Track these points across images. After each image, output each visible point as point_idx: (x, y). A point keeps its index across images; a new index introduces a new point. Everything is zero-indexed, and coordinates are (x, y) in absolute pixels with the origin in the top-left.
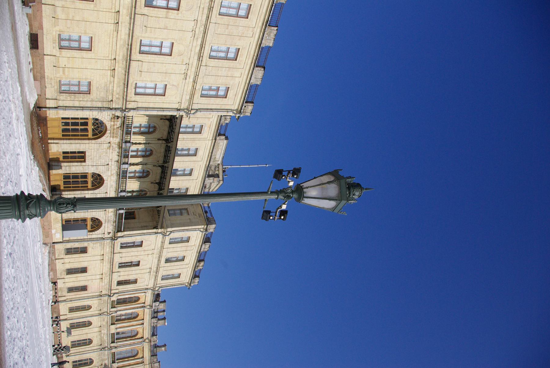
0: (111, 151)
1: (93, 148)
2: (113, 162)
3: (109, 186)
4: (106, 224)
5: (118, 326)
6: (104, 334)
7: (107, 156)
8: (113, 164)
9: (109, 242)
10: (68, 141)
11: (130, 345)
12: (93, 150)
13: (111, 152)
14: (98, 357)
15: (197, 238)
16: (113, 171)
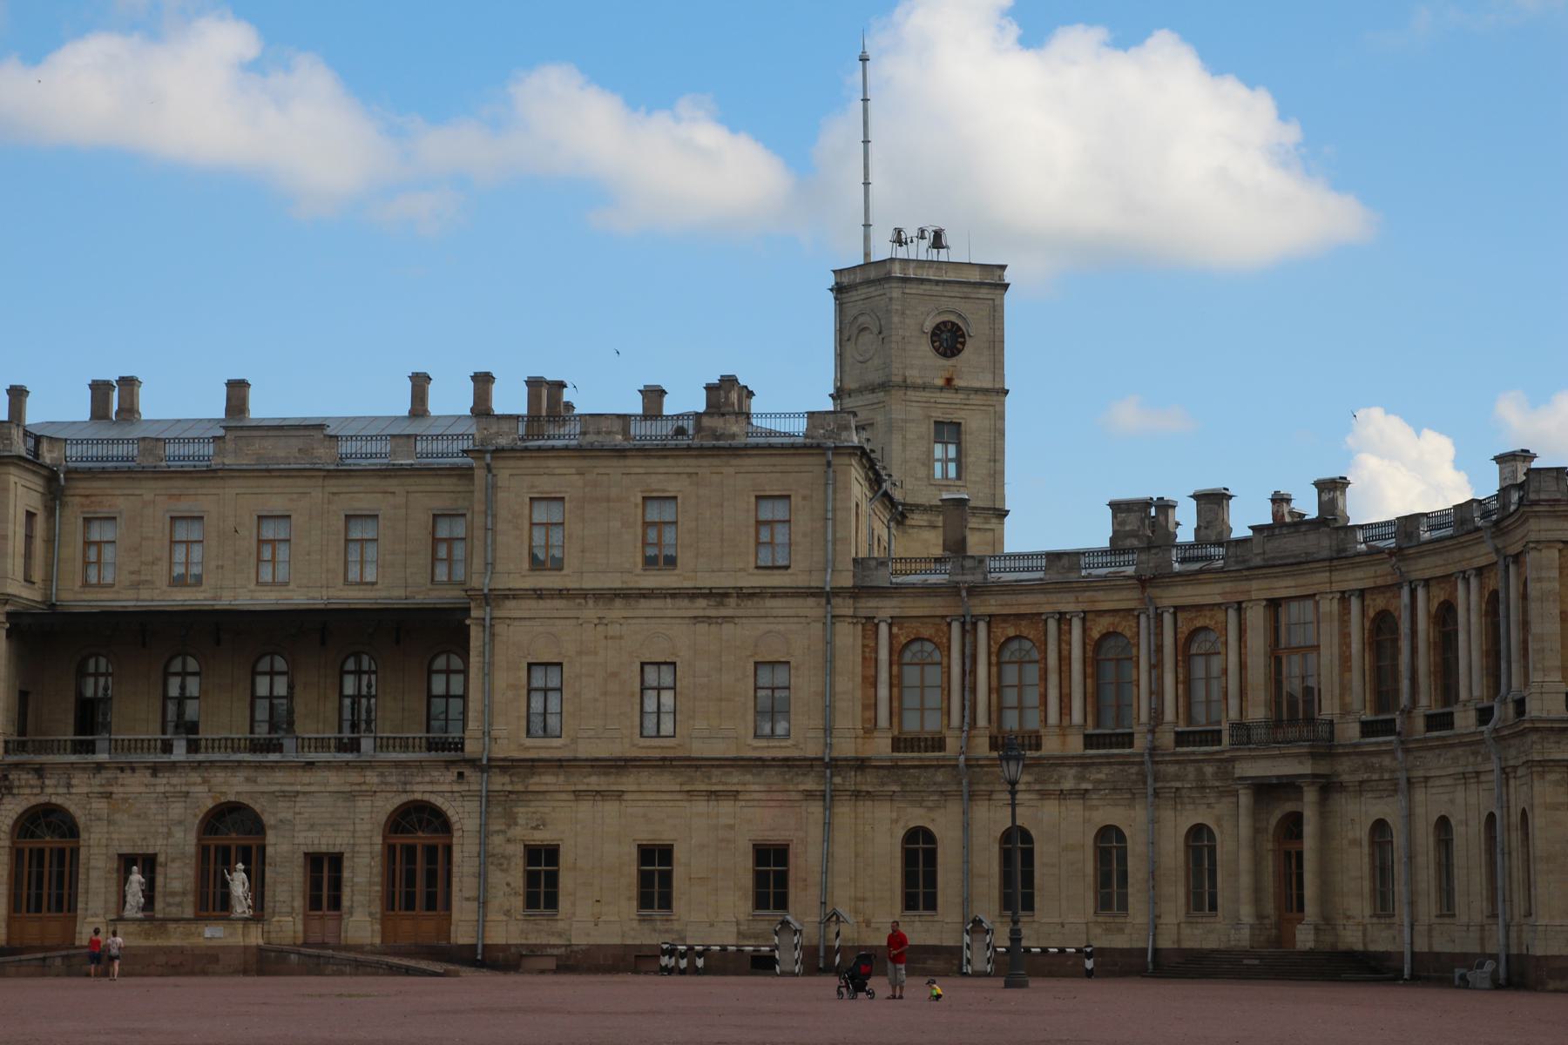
0: (115, 789)
1: (106, 836)
2: (158, 781)
3: (247, 788)
4: (415, 788)
5: (1053, 717)
6: (1082, 779)
7: (136, 798)
8: (164, 781)
9: (511, 776)
10: (81, 899)
11: (1156, 666)
12: (115, 836)
13: (121, 789)
14: (1188, 807)
15: (542, 471)
16: (192, 780)
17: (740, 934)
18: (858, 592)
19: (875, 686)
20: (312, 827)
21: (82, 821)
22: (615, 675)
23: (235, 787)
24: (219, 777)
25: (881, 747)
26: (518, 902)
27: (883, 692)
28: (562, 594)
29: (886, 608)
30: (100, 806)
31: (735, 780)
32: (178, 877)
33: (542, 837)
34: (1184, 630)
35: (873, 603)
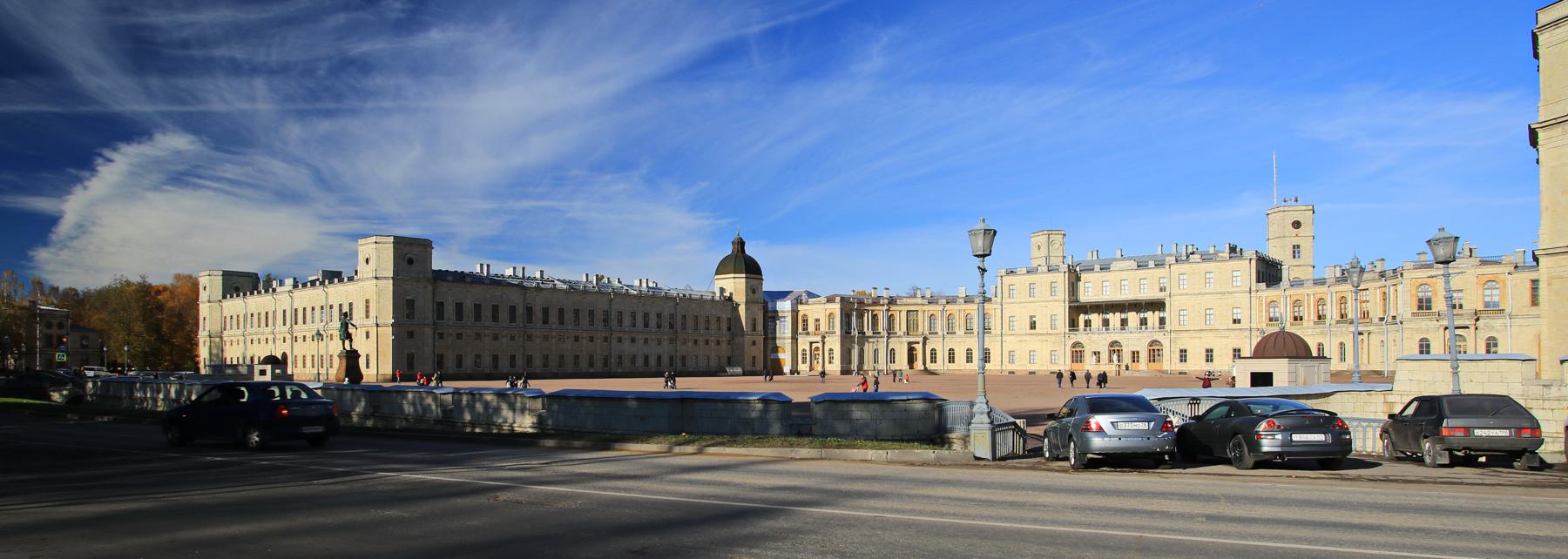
21: (1085, 345)
26: (1178, 361)
30: (1088, 341)
31: (1227, 333)
32: (1104, 356)
33: (1183, 347)
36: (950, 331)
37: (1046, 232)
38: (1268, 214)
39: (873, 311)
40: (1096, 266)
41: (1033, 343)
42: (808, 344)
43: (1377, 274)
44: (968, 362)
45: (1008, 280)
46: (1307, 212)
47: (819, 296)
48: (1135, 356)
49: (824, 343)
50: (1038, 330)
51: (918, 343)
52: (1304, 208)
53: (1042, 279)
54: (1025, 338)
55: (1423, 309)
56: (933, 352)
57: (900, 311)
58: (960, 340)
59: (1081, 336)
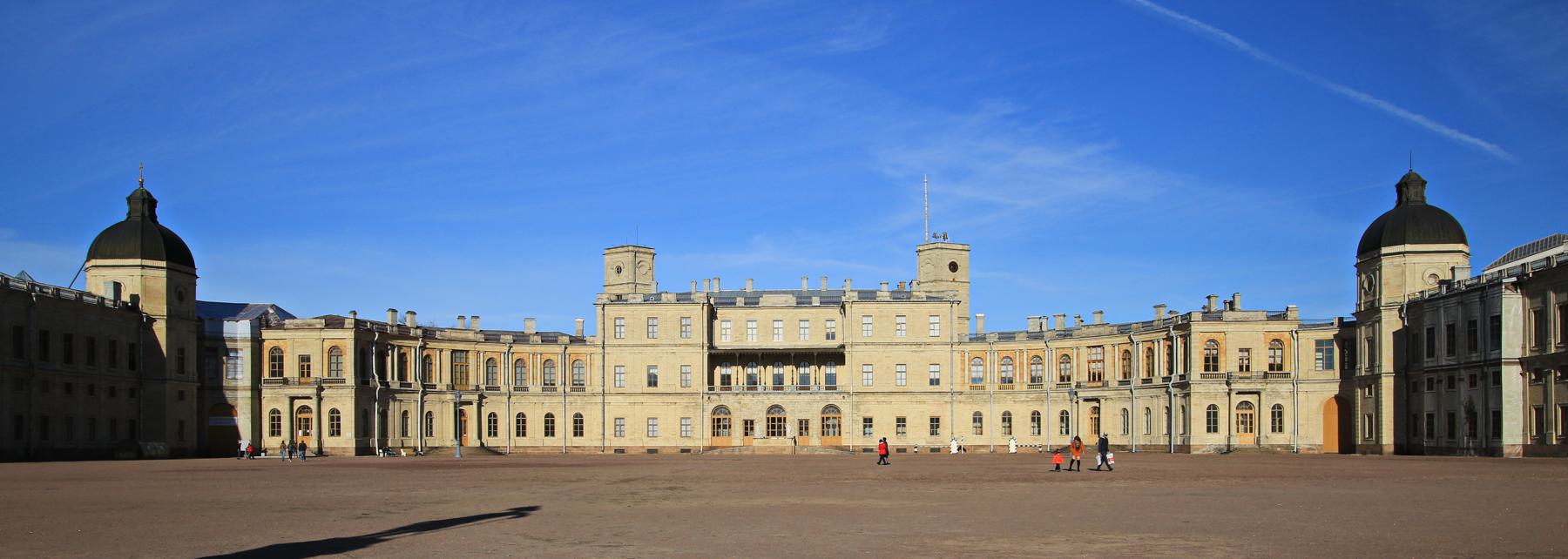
5: (1018, 380)
17: (927, 442)
18: (960, 343)
19: (964, 370)
20: (801, 412)
21: (732, 410)
22: (888, 368)
23: (777, 399)
24: (772, 397)
25: (966, 388)
27: (967, 372)
28: (873, 344)
29: (968, 348)
30: (737, 405)
31: (924, 397)
33: (868, 415)
34: (1059, 355)
35: (964, 347)
36: (518, 385)
37: (631, 248)
38: (920, 251)
39: (400, 347)
40: (738, 299)
41: (654, 406)
42: (287, 402)
43: (1116, 328)
44: (546, 435)
45: (612, 311)
46: (964, 252)
47: (294, 318)
48: (804, 426)
49: (320, 399)
50: (660, 388)
51: (470, 403)
52: (960, 247)
53: (669, 313)
54: (641, 399)
55: (1209, 370)
56: (493, 419)
57: (441, 351)
58: (534, 399)
59: (728, 400)
